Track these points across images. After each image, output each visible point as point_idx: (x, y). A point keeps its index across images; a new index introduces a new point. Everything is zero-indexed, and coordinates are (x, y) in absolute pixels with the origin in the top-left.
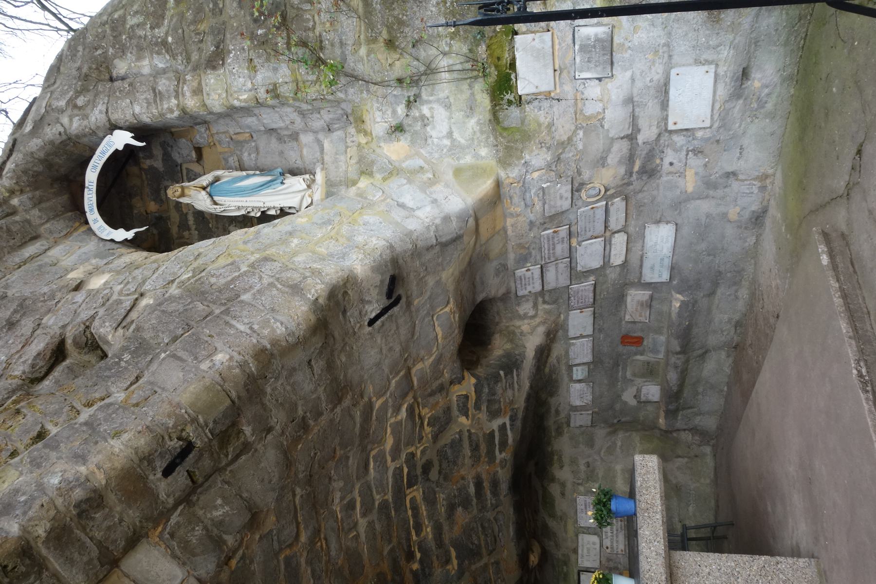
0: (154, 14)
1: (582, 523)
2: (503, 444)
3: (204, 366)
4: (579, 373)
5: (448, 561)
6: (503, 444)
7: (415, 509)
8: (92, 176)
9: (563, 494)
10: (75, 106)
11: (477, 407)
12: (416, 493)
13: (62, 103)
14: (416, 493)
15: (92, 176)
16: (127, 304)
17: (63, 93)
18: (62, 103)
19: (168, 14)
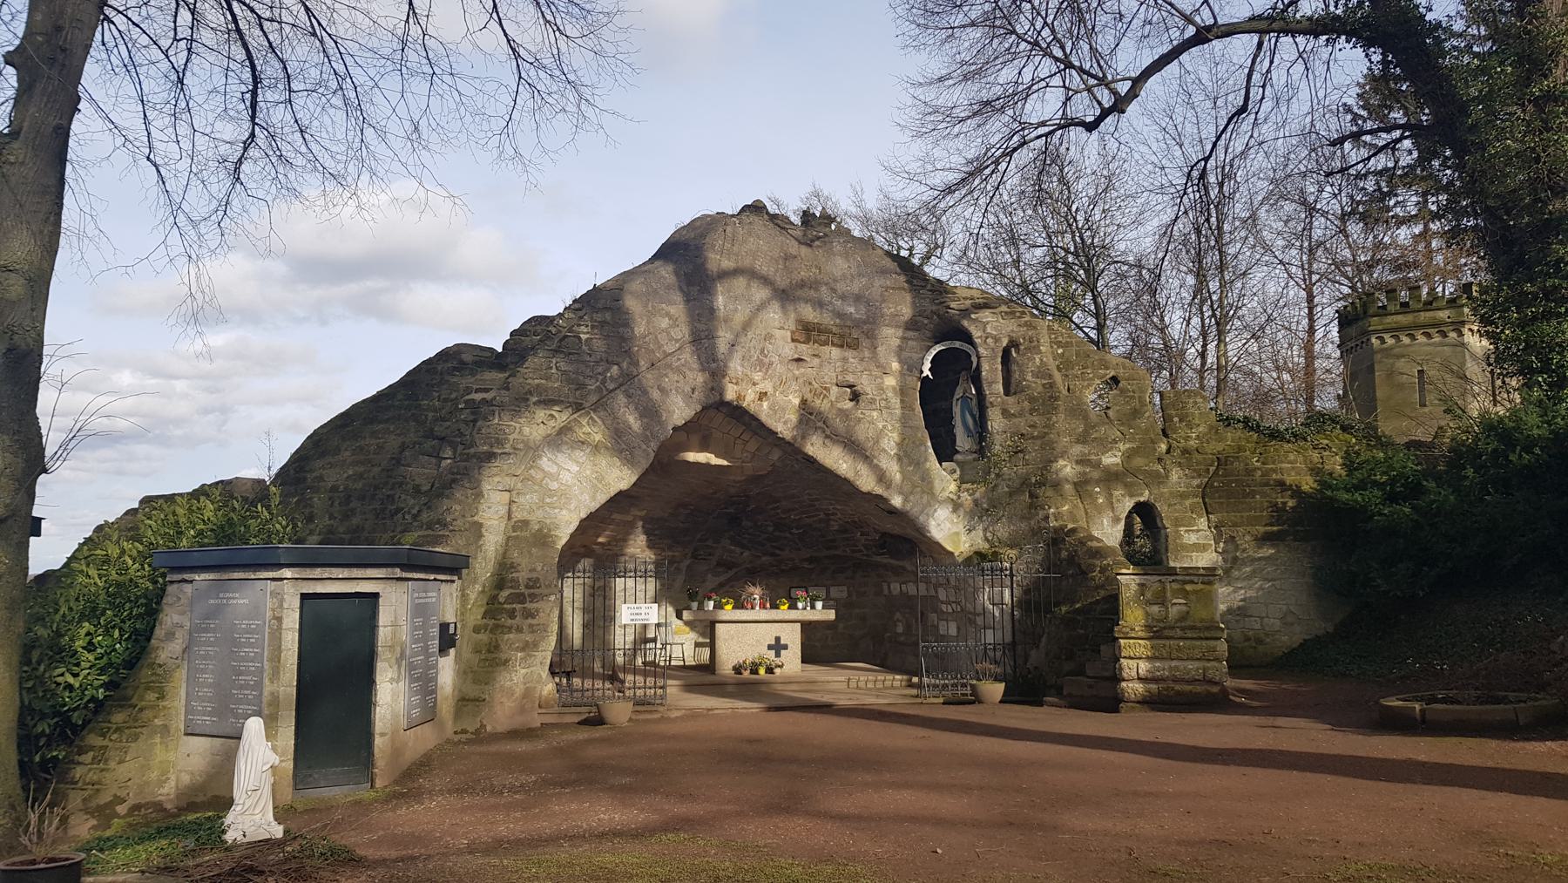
0: (1039, 372)
1: (832, 589)
2: (853, 551)
3: (841, 462)
4: (904, 587)
5: (797, 529)
6: (853, 551)
7: (816, 516)
8: (957, 344)
9: (847, 578)
10: (987, 338)
11: (866, 540)
12: (822, 516)
13: (989, 330)
14: (822, 516)
15: (957, 344)
16: (874, 407)
17: (995, 328)
18: (989, 330)
19: (1038, 381)
